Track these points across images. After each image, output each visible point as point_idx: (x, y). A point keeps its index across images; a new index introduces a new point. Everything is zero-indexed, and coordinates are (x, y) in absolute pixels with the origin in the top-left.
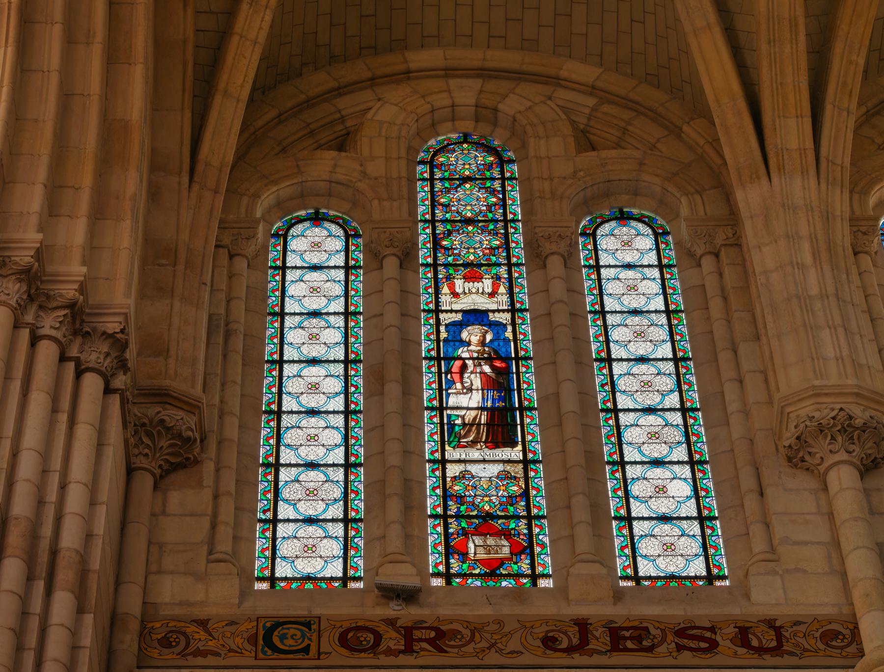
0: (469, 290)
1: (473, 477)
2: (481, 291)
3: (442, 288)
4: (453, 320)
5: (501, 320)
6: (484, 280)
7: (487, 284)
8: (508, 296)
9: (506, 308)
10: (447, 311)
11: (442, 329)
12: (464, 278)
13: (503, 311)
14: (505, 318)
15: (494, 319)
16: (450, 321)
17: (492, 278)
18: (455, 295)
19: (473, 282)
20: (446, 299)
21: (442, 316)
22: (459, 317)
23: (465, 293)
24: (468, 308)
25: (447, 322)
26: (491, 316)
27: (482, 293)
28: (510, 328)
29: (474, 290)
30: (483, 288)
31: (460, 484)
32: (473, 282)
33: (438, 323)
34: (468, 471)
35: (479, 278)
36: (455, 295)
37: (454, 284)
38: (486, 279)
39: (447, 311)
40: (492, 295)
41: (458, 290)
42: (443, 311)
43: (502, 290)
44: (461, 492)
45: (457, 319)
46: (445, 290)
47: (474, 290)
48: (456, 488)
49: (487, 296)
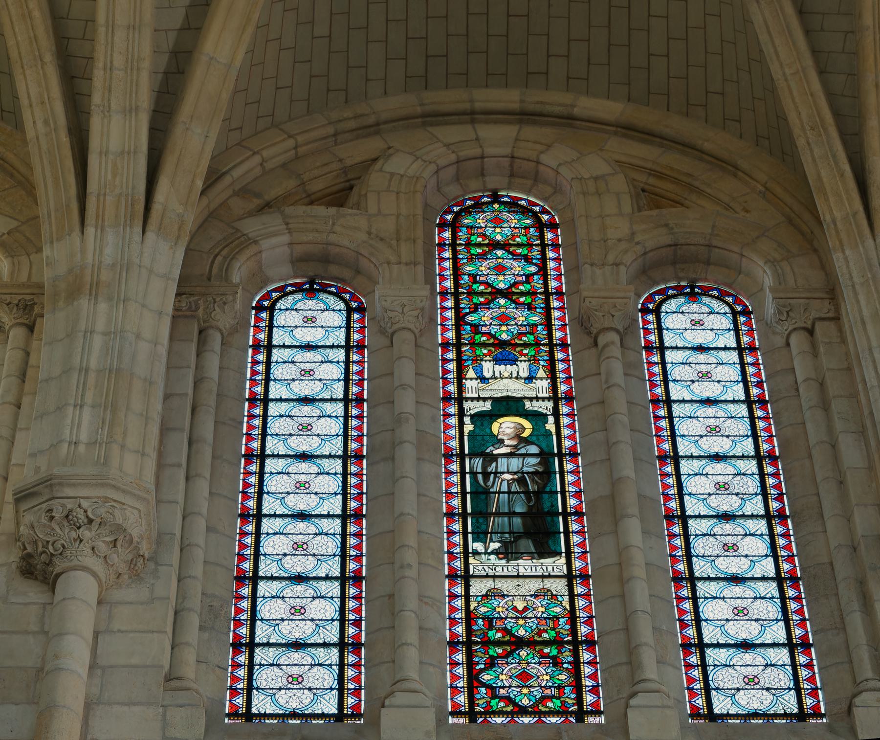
0: (500, 374)
1: (503, 596)
2: (514, 375)
3: (467, 372)
4: (480, 409)
5: (540, 410)
6: (518, 363)
7: (523, 368)
8: (549, 381)
9: (547, 395)
10: (472, 399)
11: (467, 420)
13: (543, 399)
14: (546, 407)
15: (531, 408)
16: (476, 410)
17: (529, 361)
18: (483, 379)
19: (506, 365)
20: (471, 386)
21: (466, 405)
22: (487, 406)
24: (500, 395)
25: (472, 412)
26: (528, 404)
28: (551, 419)
29: (506, 374)
30: (518, 372)
32: (506, 365)
33: (461, 414)
35: (514, 361)
36: (483, 379)
39: (472, 399)
40: (530, 379)
41: (487, 375)
42: (467, 399)
43: (541, 373)
44: (488, 614)
45: (485, 409)
46: (471, 374)
47: (506, 374)
48: (483, 609)
49: (523, 381)
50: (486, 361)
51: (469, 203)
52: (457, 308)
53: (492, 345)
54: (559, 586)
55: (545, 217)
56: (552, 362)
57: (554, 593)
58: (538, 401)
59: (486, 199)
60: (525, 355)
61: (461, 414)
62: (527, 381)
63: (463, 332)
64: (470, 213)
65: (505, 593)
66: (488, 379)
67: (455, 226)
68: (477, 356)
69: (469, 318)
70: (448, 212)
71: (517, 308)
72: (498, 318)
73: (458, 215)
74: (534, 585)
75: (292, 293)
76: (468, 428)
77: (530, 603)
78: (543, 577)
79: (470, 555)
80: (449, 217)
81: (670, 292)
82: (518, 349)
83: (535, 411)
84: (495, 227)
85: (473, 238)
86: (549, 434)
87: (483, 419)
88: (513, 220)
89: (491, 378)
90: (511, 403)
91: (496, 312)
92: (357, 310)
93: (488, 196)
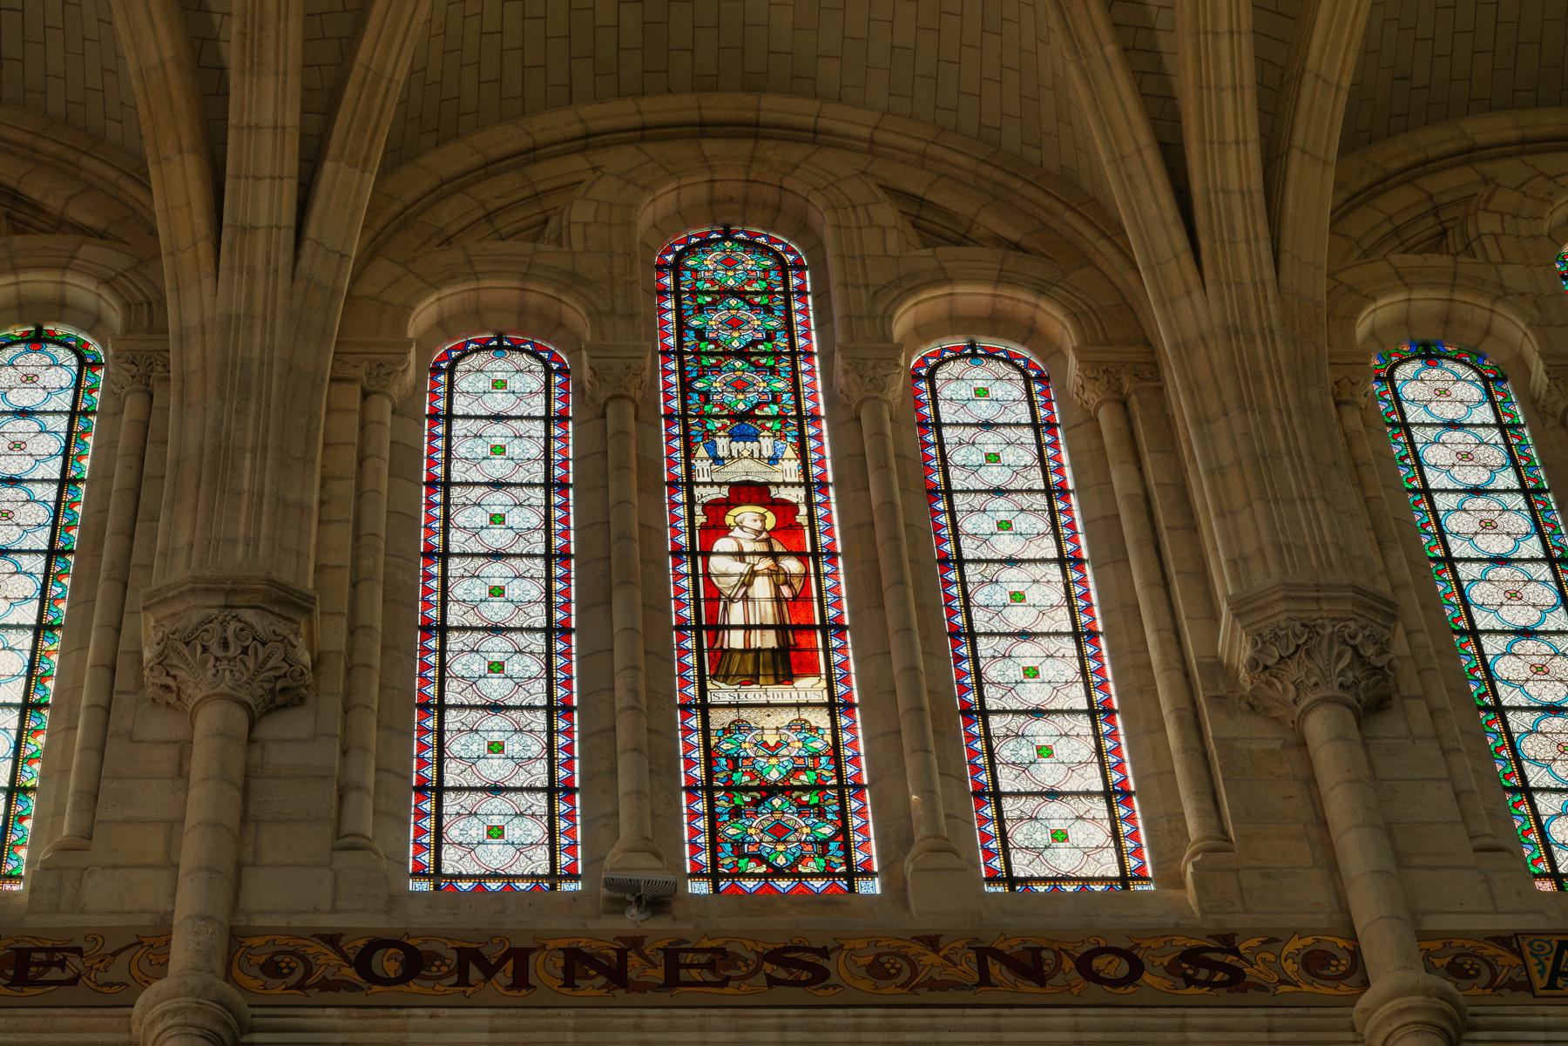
0: (739, 453)
1: (751, 729)
2: (756, 455)
3: (697, 450)
4: (714, 497)
5: (789, 498)
6: (761, 439)
7: (766, 445)
8: (799, 461)
9: (796, 480)
10: (704, 484)
11: (698, 510)
12: (730, 435)
13: (793, 485)
14: (795, 495)
15: (778, 496)
16: (709, 498)
17: (775, 436)
18: (717, 460)
19: (745, 442)
20: (702, 466)
21: (697, 491)
22: (725, 491)
23: (733, 458)
24: (737, 479)
25: (705, 500)
26: (774, 492)
27: (759, 459)
28: (803, 510)
29: (746, 453)
30: (760, 451)
31: (732, 740)
32: (745, 442)
33: (691, 502)
34: (743, 721)
35: (755, 437)
36: (717, 460)
37: (715, 444)
38: (764, 437)
39: (704, 484)
40: (774, 460)
41: (721, 453)
42: (698, 484)
43: (790, 453)
44: (732, 752)
45: (720, 496)
46: (702, 452)
47: (746, 453)
48: (725, 746)
49: (766, 461)
50: (720, 437)
51: (694, 240)
52: (682, 372)
53: (727, 417)
54: (821, 719)
55: (790, 258)
56: (801, 441)
57: (814, 724)
58: (786, 487)
59: (714, 236)
60: (769, 429)
61: (691, 502)
62: (771, 462)
63: (690, 402)
64: (695, 254)
65: (753, 725)
66: (723, 459)
67: (677, 268)
68: (708, 431)
69: (698, 385)
70: (667, 252)
71: (757, 372)
72: (732, 384)
73: (679, 256)
74: (790, 715)
75: (477, 351)
76: (700, 519)
77: (783, 738)
78: (798, 706)
79: (708, 678)
80: (670, 258)
81: (947, 354)
82: (759, 422)
83: (783, 500)
84: (726, 270)
85: (699, 284)
86: (801, 526)
87: (717, 510)
88: (750, 261)
89: (728, 458)
90: (753, 489)
91: (729, 377)
92: (560, 372)
93: (718, 233)
